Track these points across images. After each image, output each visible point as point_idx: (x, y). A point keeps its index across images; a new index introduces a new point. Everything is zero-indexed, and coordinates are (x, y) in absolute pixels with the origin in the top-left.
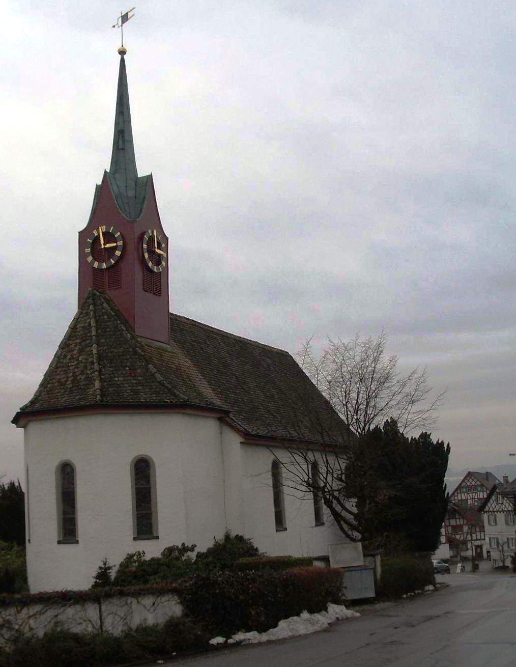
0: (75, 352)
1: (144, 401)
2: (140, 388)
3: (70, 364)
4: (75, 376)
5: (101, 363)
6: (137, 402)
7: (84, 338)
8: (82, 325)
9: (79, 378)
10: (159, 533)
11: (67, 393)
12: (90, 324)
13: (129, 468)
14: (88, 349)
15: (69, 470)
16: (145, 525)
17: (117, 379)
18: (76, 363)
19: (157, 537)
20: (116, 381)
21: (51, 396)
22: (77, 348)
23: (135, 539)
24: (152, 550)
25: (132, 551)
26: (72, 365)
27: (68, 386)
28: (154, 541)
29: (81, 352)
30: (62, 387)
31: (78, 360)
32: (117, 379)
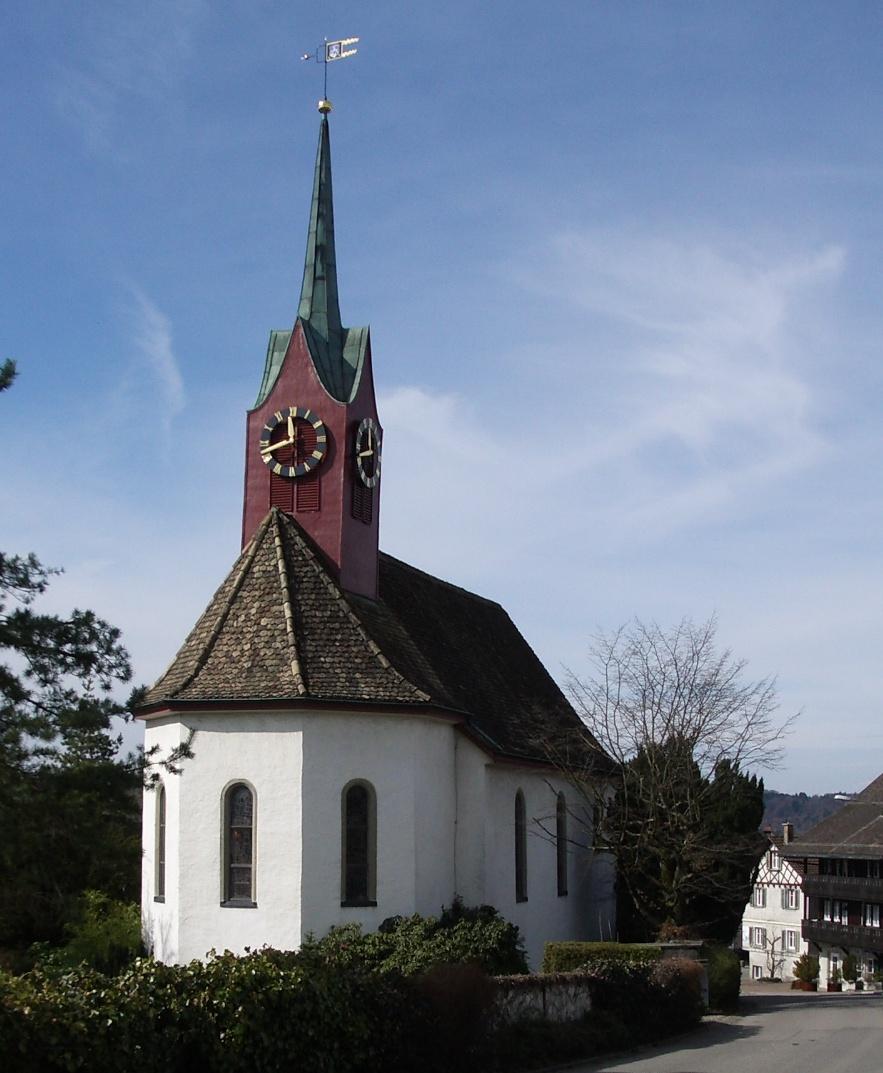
0: (253, 611)
1: (367, 697)
2: (358, 675)
3: (245, 630)
4: (255, 651)
5: (299, 632)
6: (358, 699)
7: (267, 590)
8: (263, 568)
9: (262, 654)
10: (378, 897)
11: (244, 675)
12: (276, 566)
13: (339, 798)
14: (276, 608)
15: (243, 795)
16: (357, 886)
17: (322, 659)
18: (255, 628)
19: (374, 904)
20: (322, 663)
21: (216, 677)
22: (256, 605)
23: (343, 905)
24: (367, 921)
25: (339, 923)
26: (249, 632)
27: (245, 665)
28: (370, 909)
29: (262, 612)
30: (233, 665)
31: (259, 624)
32: (322, 659)
